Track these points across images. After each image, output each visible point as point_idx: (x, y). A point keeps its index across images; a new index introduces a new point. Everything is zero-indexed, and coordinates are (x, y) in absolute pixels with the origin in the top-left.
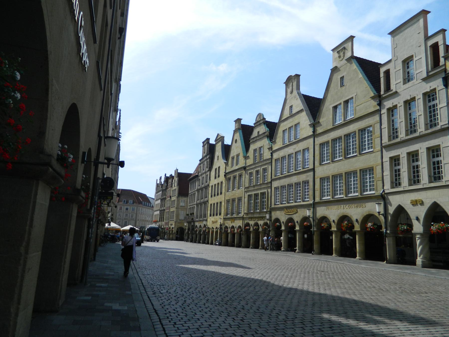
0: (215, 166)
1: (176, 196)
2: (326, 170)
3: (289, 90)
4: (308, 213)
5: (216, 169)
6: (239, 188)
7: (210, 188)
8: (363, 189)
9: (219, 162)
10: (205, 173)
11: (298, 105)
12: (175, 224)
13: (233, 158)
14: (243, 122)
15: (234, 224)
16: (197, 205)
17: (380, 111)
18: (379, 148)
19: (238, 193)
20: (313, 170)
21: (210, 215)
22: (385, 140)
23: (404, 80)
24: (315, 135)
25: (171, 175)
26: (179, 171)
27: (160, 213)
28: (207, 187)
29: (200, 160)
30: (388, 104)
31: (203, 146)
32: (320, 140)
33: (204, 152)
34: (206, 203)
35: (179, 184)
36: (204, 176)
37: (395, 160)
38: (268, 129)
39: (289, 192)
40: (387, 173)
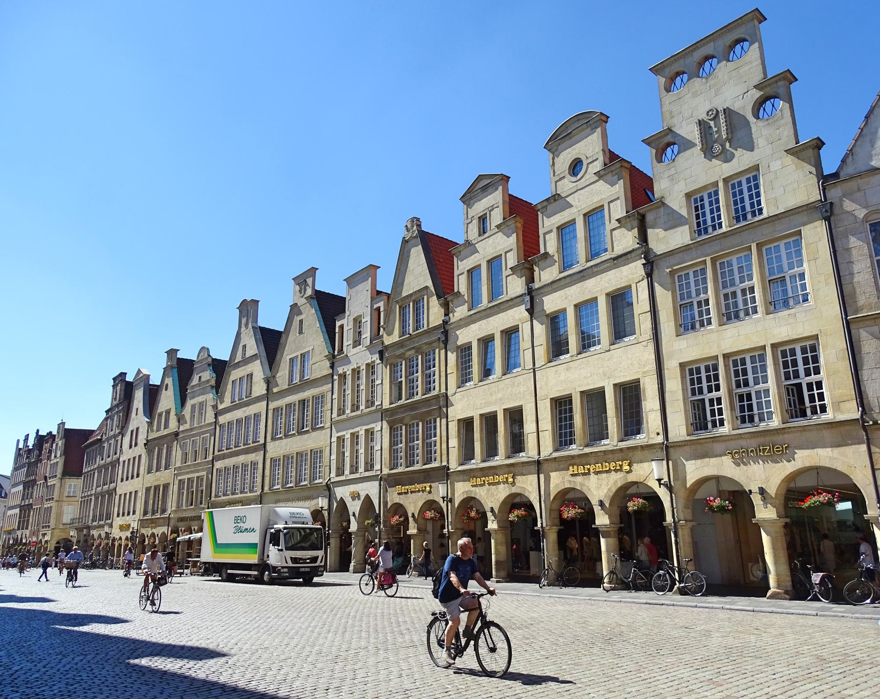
0: (132, 426)
1: (59, 476)
5: (132, 431)
6: (166, 468)
7: (121, 467)
9: (138, 419)
10: (115, 436)
11: (252, 346)
13: (160, 415)
14: (180, 355)
15: (155, 531)
16: (97, 496)
18: (328, 425)
19: (164, 476)
20: (265, 444)
21: (118, 515)
22: (335, 415)
23: (355, 342)
24: (268, 396)
25: (51, 433)
28: (115, 464)
29: (107, 412)
31: (113, 386)
33: (114, 399)
34: (112, 493)
35: (66, 452)
36: (112, 441)
37: (341, 440)
38: (214, 375)
40: (334, 457)
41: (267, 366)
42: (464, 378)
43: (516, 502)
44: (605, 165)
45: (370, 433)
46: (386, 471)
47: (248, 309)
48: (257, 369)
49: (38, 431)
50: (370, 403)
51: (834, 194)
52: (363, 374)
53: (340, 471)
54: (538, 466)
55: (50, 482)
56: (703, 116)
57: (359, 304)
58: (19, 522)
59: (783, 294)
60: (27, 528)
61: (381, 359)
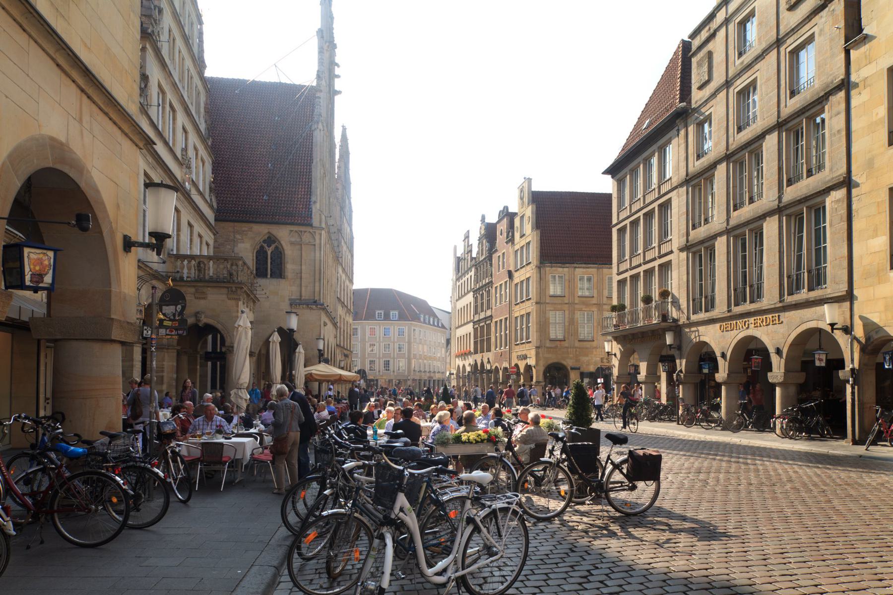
1: (533, 266)
12: (537, 354)
25: (506, 208)
26: (536, 188)
27: (475, 330)
35: (540, 223)
49: (483, 218)
55: (518, 277)
58: (476, 343)
60: (489, 350)
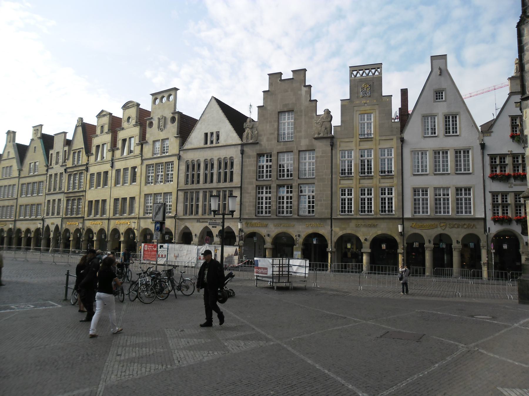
2: (23, 200)
3: (9, 140)
4: (11, 226)
8: (37, 215)
17: (47, 174)
20: (17, 199)
22: (47, 191)
24: (19, 177)
30: (51, 172)
32: (23, 181)
39: (7, 209)
40: (46, 208)
41: (20, 164)
42: (91, 187)
43: (102, 231)
44: (136, 122)
45: (59, 200)
46: (64, 216)
47: (11, 135)
48: (14, 164)
50: (60, 188)
51: (181, 153)
52: (58, 176)
53: (48, 214)
54: (109, 219)
56: (159, 117)
57: (58, 146)
59: (167, 179)
61: (65, 172)
